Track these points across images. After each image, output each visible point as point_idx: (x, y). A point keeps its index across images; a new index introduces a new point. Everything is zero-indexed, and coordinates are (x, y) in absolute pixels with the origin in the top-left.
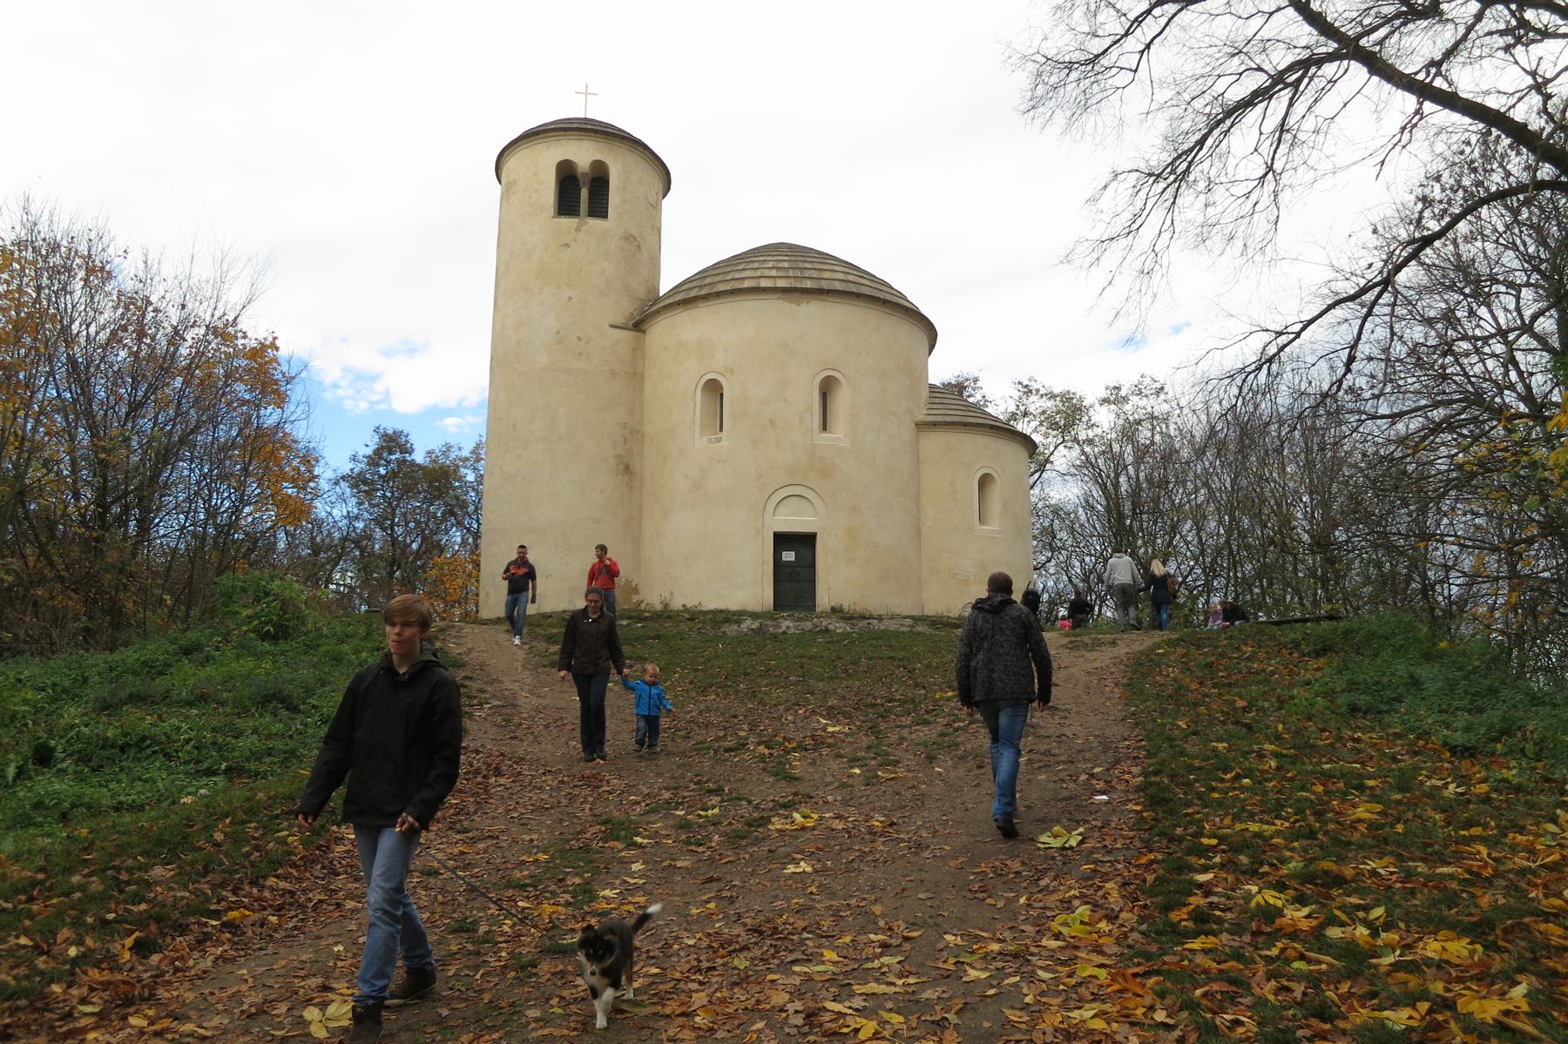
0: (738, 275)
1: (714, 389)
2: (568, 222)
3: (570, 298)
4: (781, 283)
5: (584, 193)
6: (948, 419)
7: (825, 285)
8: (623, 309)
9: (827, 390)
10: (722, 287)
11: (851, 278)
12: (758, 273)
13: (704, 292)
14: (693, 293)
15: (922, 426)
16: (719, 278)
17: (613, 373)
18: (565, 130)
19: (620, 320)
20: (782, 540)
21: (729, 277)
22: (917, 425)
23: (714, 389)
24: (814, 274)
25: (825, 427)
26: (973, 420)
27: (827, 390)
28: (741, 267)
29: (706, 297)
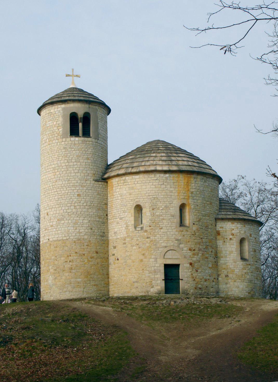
5: (80, 125)
11: (190, 163)
12: (155, 163)
14: (130, 170)
20: (167, 267)
21: (143, 164)
28: (147, 159)
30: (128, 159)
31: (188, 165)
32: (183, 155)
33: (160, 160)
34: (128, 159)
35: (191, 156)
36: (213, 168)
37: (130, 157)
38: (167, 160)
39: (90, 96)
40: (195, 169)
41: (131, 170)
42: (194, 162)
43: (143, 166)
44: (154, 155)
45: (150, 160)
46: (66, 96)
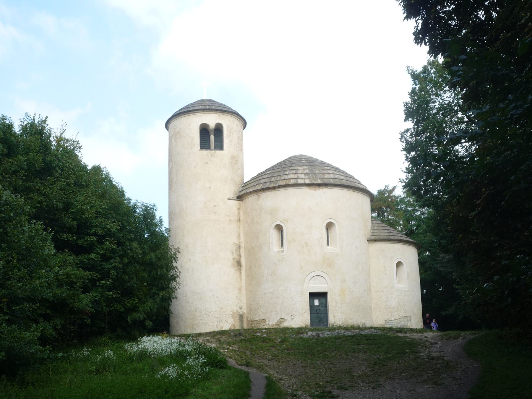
0: (287, 177)
1: (279, 228)
2: (205, 152)
3: (210, 187)
4: (307, 181)
5: (212, 137)
6: (382, 237)
7: (326, 181)
8: (232, 190)
9: (329, 226)
10: (281, 183)
11: (337, 176)
12: (296, 176)
13: (272, 186)
14: (267, 186)
15: (370, 241)
16: (278, 178)
17: (230, 220)
18: (203, 110)
19: (231, 195)
20: (313, 295)
21: (283, 178)
22: (368, 240)
23: (279, 228)
24: (321, 176)
25: (328, 245)
26: (392, 238)
27: (329, 226)
28: (287, 173)
29: (274, 188)
30: (266, 174)
31: (334, 178)
32: (328, 168)
33: (302, 173)
34: (266, 174)
35: (337, 169)
36: (362, 183)
37: (268, 172)
38: (310, 172)
39: (223, 106)
40: (344, 183)
41: (269, 185)
42: (341, 175)
43: (283, 180)
44: (296, 168)
45: (290, 173)
46: (195, 106)
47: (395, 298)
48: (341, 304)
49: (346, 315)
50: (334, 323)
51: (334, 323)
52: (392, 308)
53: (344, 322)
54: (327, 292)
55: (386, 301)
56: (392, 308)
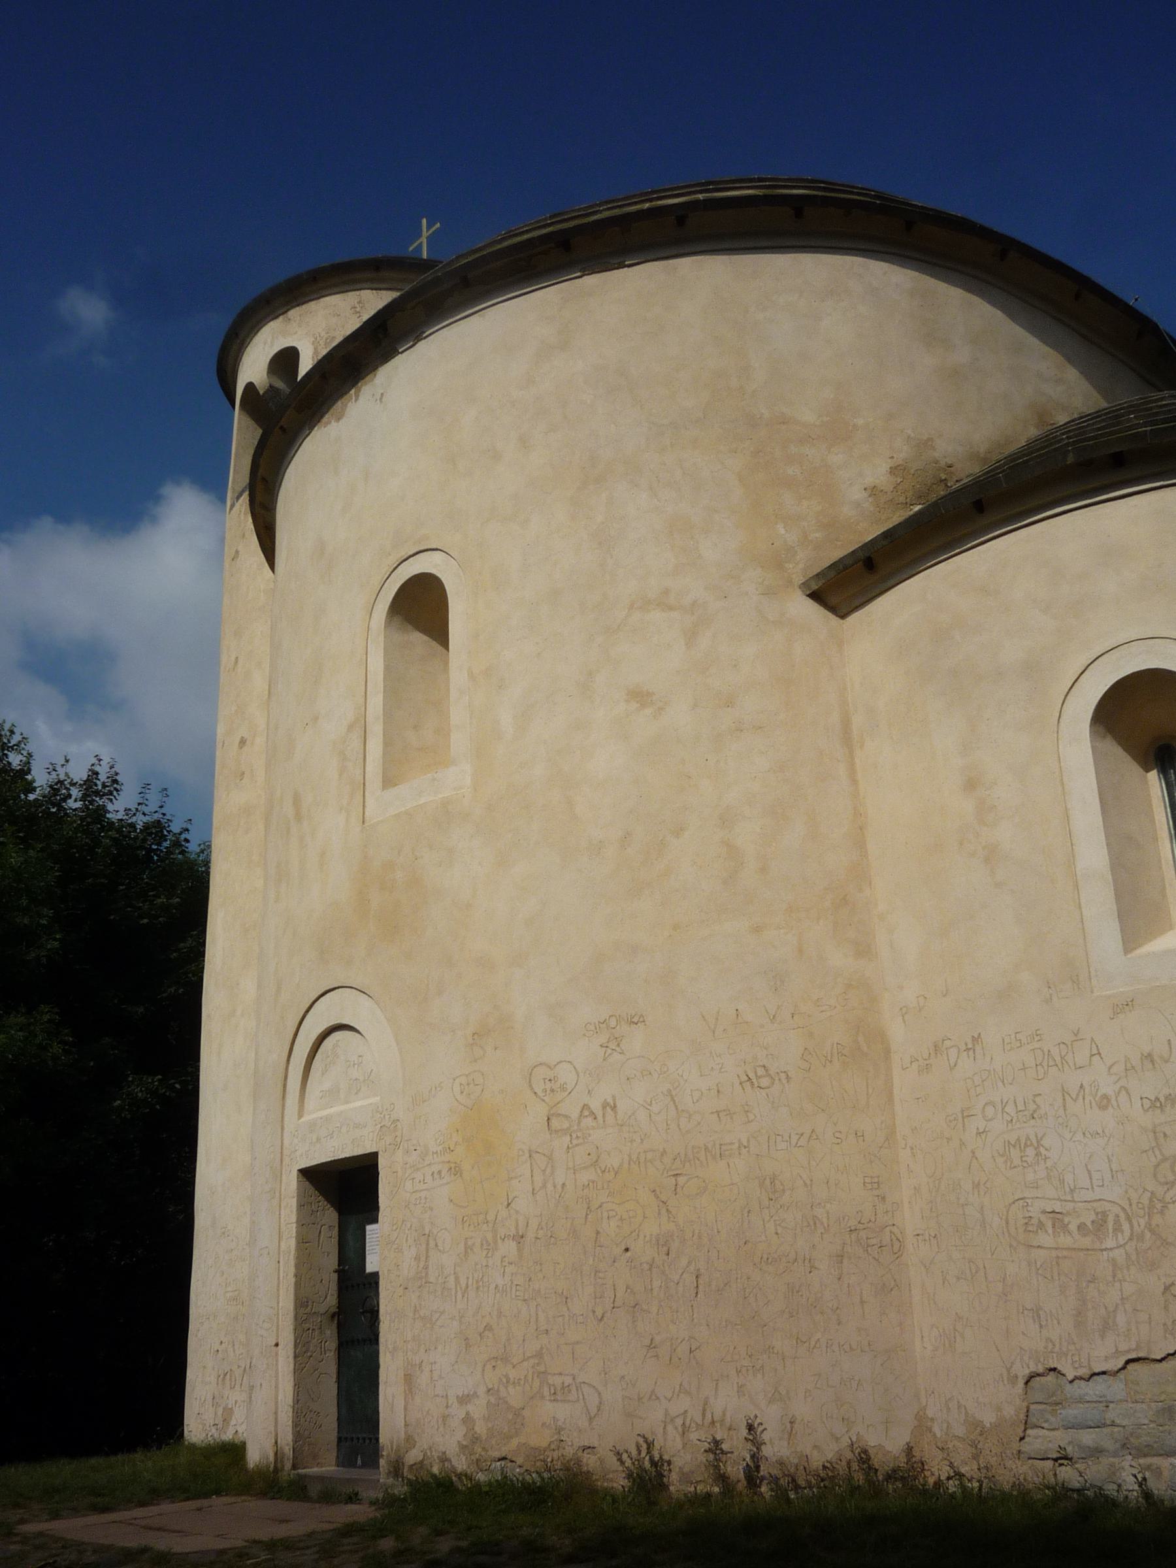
22: (815, 596)
47: (1104, 1103)
48: (468, 1249)
49: (505, 1359)
50: (410, 1441)
51: (410, 1441)
52: (1088, 1218)
53: (481, 1429)
54: (374, 1156)
55: (1015, 1153)
56: (1081, 1227)
